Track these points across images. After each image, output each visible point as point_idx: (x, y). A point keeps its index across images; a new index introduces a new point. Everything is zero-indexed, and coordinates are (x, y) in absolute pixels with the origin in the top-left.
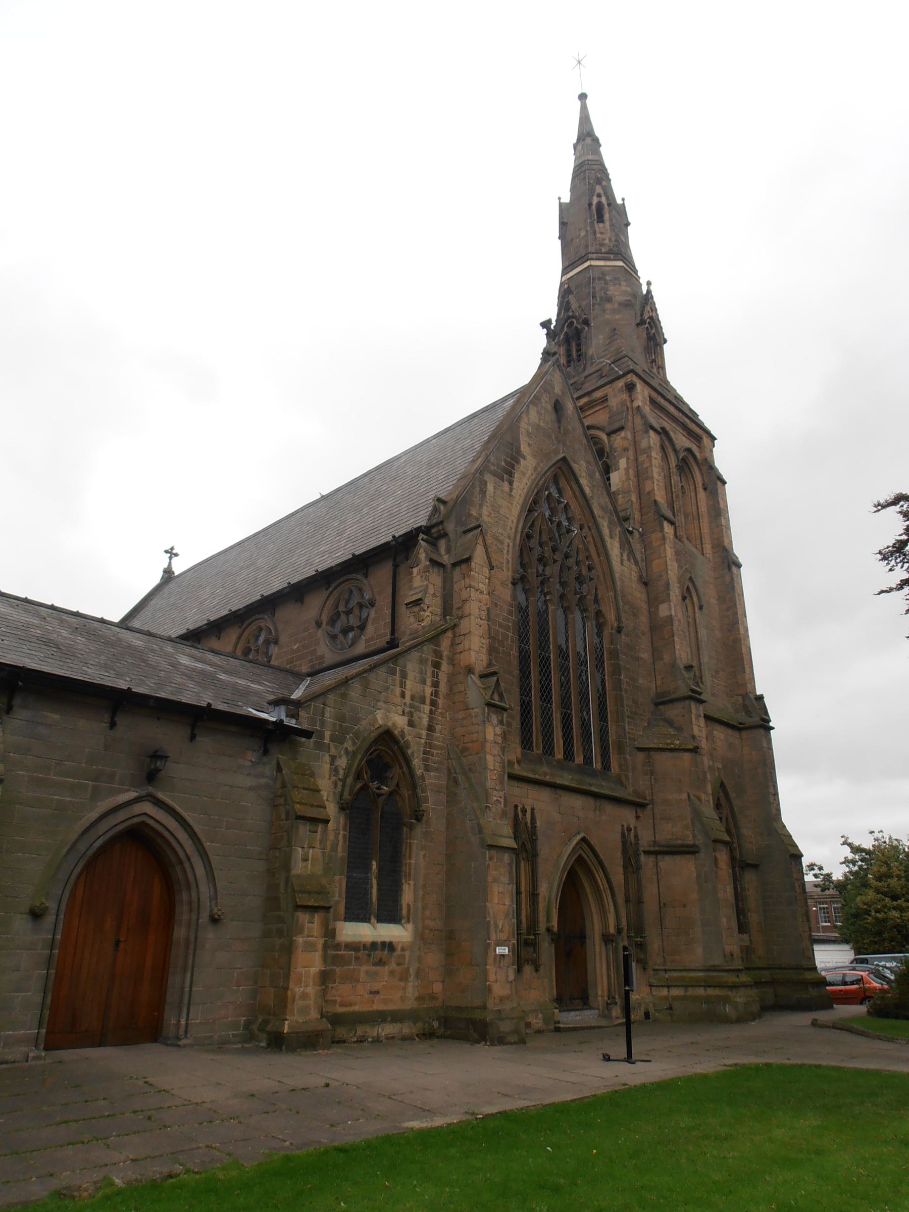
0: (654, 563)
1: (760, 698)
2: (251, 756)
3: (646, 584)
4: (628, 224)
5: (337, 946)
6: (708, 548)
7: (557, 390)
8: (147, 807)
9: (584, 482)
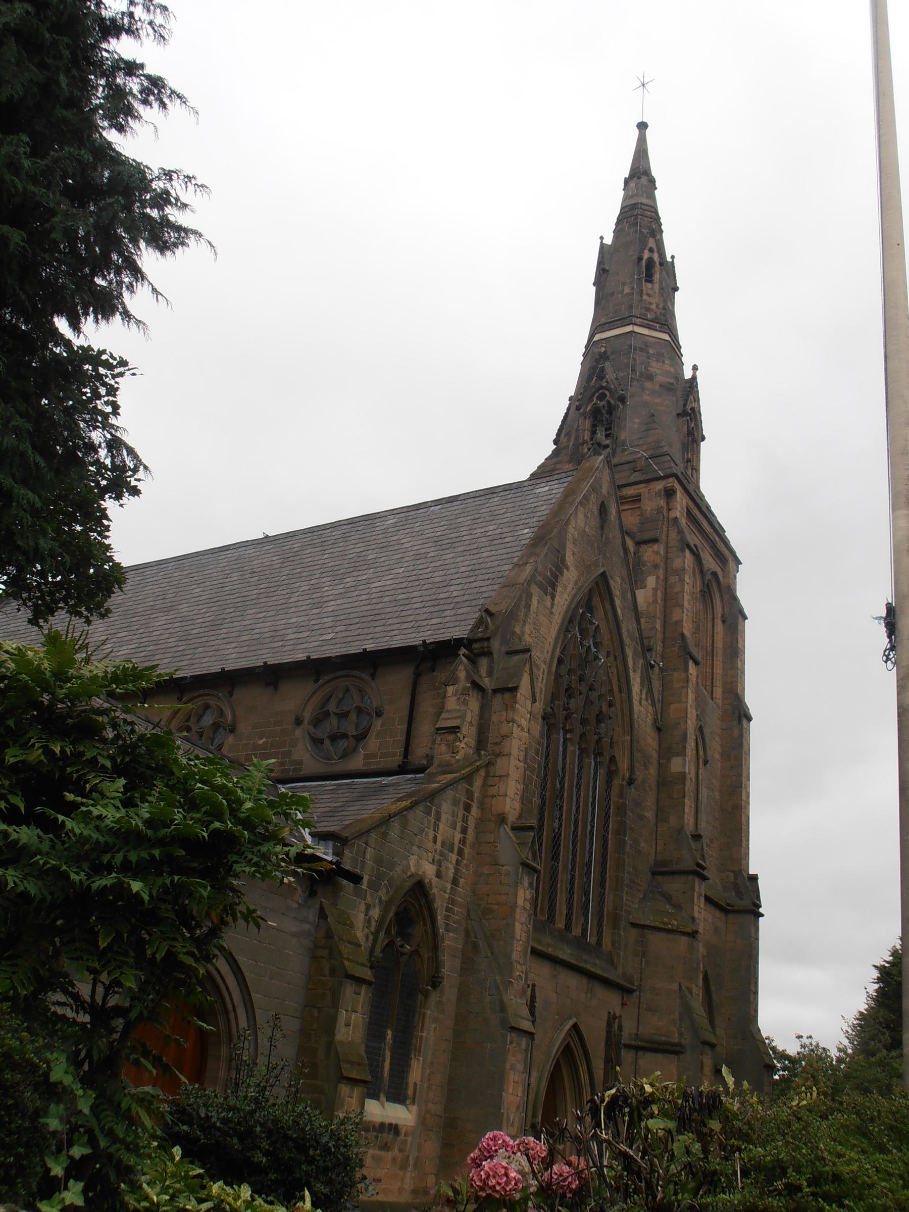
0: (672, 706)
1: (754, 878)
3: (659, 730)
4: (676, 289)
6: (718, 692)
7: (604, 490)
9: (618, 602)
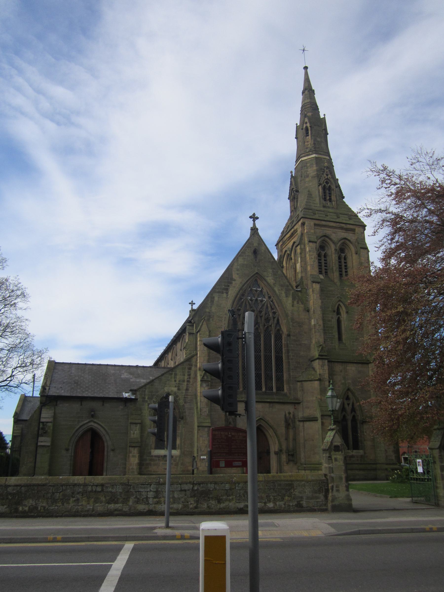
2: (121, 407)
5: (152, 456)
8: (92, 424)
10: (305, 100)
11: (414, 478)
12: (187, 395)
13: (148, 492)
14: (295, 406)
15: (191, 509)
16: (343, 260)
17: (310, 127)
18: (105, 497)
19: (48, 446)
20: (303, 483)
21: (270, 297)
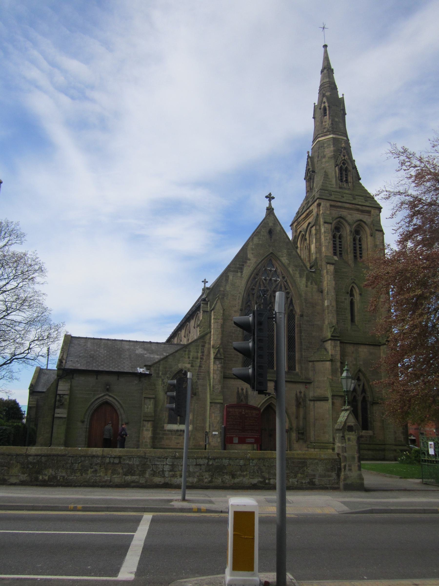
5: (165, 430)
8: (107, 397)
10: (324, 79)
11: (425, 460)
12: (200, 372)
13: (164, 465)
14: (306, 385)
15: (206, 483)
16: (357, 242)
17: (329, 106)
18: (122, 469)
19: (65, 418)
20: (316, 461)
21: (284, 278)
